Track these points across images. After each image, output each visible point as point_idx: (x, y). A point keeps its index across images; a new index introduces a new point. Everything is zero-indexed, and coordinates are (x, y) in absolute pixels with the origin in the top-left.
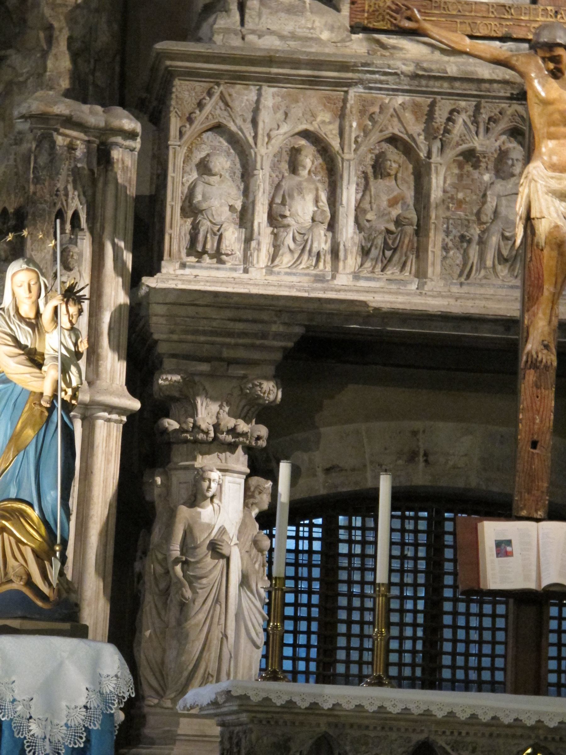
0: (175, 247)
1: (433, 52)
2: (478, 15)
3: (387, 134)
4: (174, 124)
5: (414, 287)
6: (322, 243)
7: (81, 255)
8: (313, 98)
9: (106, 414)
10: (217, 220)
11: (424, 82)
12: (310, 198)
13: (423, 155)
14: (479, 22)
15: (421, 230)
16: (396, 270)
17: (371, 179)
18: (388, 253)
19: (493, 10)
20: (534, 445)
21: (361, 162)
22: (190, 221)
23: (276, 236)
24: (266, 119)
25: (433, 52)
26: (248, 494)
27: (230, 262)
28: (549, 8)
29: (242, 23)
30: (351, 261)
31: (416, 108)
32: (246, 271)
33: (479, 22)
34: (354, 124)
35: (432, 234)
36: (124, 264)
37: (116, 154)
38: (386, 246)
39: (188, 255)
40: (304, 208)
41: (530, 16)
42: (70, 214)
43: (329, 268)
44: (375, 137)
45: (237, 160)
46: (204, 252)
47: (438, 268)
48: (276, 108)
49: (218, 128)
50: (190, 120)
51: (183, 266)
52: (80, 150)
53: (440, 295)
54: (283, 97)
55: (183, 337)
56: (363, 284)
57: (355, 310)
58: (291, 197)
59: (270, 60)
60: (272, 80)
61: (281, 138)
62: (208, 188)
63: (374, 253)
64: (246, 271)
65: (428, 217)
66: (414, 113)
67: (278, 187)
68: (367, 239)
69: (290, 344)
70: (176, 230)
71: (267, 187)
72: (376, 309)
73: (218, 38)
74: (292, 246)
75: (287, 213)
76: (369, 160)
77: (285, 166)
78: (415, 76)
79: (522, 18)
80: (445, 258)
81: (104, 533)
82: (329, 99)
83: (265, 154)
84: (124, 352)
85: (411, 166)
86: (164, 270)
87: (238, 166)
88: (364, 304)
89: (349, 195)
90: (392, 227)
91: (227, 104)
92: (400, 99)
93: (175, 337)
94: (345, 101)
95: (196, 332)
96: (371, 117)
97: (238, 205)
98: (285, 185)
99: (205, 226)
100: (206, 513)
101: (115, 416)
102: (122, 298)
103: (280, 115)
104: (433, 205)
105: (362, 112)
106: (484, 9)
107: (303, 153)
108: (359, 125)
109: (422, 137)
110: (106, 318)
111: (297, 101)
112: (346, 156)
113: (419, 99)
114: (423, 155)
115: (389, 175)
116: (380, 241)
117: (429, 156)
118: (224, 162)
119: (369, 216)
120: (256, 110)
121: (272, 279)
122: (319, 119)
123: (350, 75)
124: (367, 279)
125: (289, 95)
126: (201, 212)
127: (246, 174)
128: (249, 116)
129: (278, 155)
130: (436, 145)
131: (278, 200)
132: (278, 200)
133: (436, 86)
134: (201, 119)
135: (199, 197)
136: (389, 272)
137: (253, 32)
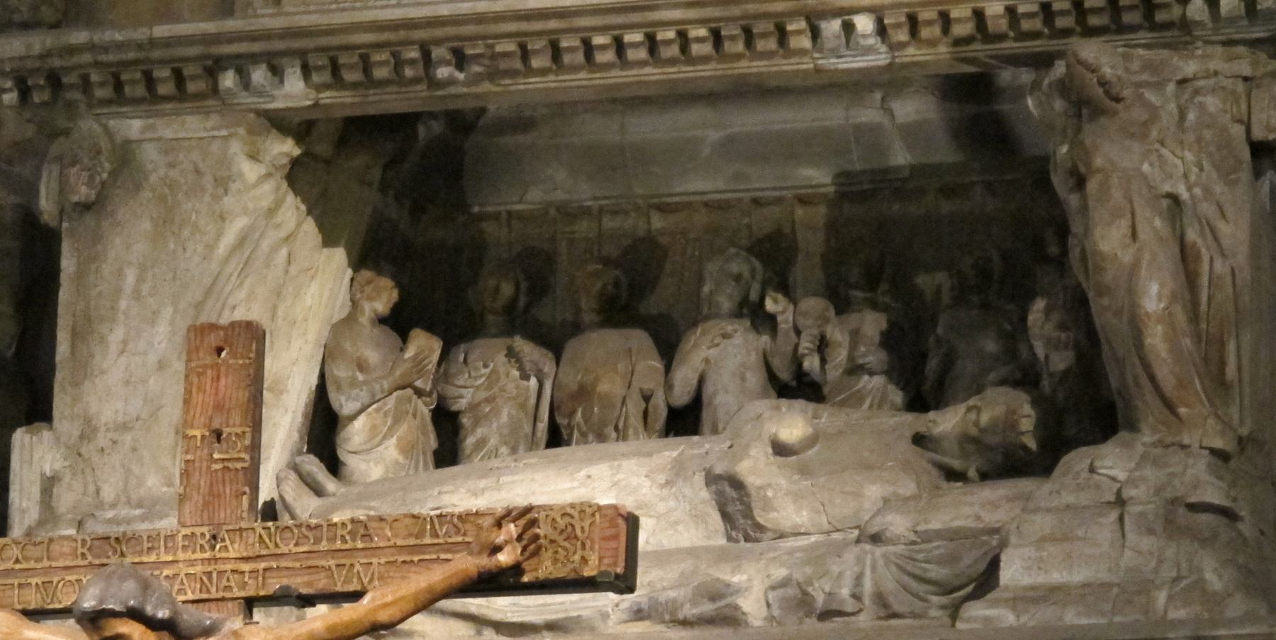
1: (479, 633)
2: (54, 564)
14: (55, 580)
19: (344, 533)
25: (479, 633)
28: (198, 531)
33: (55, 580)
41: (175, 554)
79: (145, 559)
106: (66, 549)
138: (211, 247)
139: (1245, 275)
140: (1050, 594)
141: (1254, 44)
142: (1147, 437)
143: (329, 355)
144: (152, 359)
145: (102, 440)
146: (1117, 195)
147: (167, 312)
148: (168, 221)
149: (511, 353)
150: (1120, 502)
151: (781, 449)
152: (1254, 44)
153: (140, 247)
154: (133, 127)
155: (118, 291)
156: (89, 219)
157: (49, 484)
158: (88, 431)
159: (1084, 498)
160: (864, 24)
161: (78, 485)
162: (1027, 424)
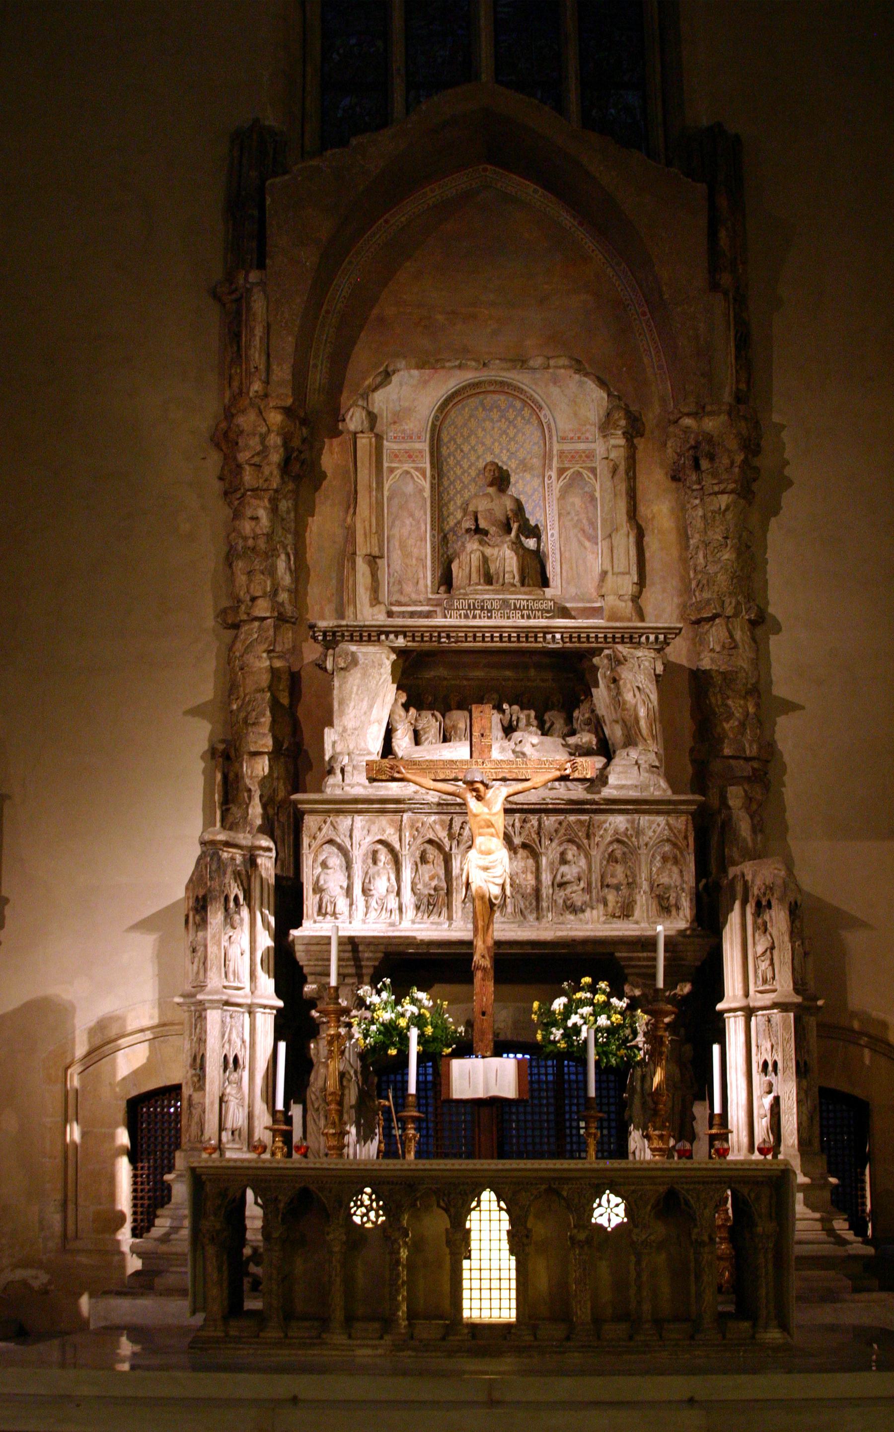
0: (310, 912)
3: (426, 838)
4: (306, 841)
5: (446, 926)
6: (393, 903)
8: (383, 821)
9: (262, 1010)
10: (333, 894)
11: (445, 807)
12: (385, 878)
13: (447, 849)
15: (449, 893)
16: (436, 917)
17: (419, 865)
18: (431, 908)
21: (413, 855)
22: (318, 896)
23: (367, 901)
24: (357, 834)
27: (341, 918)
29: (343, 780)
30: (410, 913)
31: (442, 822)
32: (350, 923)
34: (407, 834)
35: (454, 895)
36: (269, 923)
38: (429, 904)
39: (318, 915)
40: (382, 884)
43: (398, 917)
44: (420, 841)
45: (343, 859)
46: (326, 913)
47: (460, 914)
48: (363, 828)
49: (331, 842)
50: (315, 838)
51: (315, 922)
53: (460, 930)
54: (367, 821)
55: (316, 963)
56: (417, 926)
57: (409, 941)
58: (374, 878)
59: (356, 801)
60: (360, 812)
61: (366, 845)
62: (327, 876)
63: (422, 908)
64: (350, 923)
65: (452, 885)
66: (442, 825)
67: (367, 873)
68: (419, 900)
69: (377, 964)
70: (310, 901)
71: (361, 874)
72: (421, 940)
73: (328, 790)
74: (376, 907)
75: (372, 888)
76: (418, 854)
77: (370, 861)
78: (439, 804)
80: (464, 908)
82: (392, 820)
83: (358, 855)
84: (272, 974)
85: (442, 857)
86: (304, 925)
87: (344, 862)
88: (414, 938)
89: (407, 874)
90: (432, 892)
91: (334, 827)
92: (433, 818)
93: (312, 963)
94: (401, 821)
96: (417, 830)
97: (345, 885)
98: (371, 872)
99: (326, 898)
101: (268, 1011)
102: (271, 943)
103: (365, 832)
104: (454, 878)
105: (412, 827)
107: (379, 853)
108: (410, 834)
109: (447, 839)
111: (374, 823)
112: (404, 853)
113: (444, 817)
114: (447, 849)
115: (428, 862)
116: (425, 901)
117: (451, 849)
118: (336, 861)
119: (419, 887)
120: (351, 830)
121: (365, 926)
122: (387, 832)
123: (402, 806)
124: (420, 923)
125: (370, 820)
126: (324, 890)
127: (349, 867)
128: (348, 834)
129: (366, 855)
130: (455, 843)
131: (367, 881)
132: (367, 881)
133: (452, 809)
134: (321, 837)
135: (322, 882)
136: (432, 918)
137: (349, 785)
138: (378, 682)
139: (657, 708)
140: (622, 787)
141: (654, 649)
142: (640, 747)
144: (363, 711)
145: (349, 732)
146: (629, 686)
147: (366, 699)
148: (365, 675)
149: (433, 715)
150: (637, 763)
151: (533, 746)
152: (654, 649)
153: (357, 681)
155: (351, 692)
156: (342, 672)
157: (334, 743)
158: (345, 730)
159: (628, 763)
161: (342, 744)
162: (594, 743)
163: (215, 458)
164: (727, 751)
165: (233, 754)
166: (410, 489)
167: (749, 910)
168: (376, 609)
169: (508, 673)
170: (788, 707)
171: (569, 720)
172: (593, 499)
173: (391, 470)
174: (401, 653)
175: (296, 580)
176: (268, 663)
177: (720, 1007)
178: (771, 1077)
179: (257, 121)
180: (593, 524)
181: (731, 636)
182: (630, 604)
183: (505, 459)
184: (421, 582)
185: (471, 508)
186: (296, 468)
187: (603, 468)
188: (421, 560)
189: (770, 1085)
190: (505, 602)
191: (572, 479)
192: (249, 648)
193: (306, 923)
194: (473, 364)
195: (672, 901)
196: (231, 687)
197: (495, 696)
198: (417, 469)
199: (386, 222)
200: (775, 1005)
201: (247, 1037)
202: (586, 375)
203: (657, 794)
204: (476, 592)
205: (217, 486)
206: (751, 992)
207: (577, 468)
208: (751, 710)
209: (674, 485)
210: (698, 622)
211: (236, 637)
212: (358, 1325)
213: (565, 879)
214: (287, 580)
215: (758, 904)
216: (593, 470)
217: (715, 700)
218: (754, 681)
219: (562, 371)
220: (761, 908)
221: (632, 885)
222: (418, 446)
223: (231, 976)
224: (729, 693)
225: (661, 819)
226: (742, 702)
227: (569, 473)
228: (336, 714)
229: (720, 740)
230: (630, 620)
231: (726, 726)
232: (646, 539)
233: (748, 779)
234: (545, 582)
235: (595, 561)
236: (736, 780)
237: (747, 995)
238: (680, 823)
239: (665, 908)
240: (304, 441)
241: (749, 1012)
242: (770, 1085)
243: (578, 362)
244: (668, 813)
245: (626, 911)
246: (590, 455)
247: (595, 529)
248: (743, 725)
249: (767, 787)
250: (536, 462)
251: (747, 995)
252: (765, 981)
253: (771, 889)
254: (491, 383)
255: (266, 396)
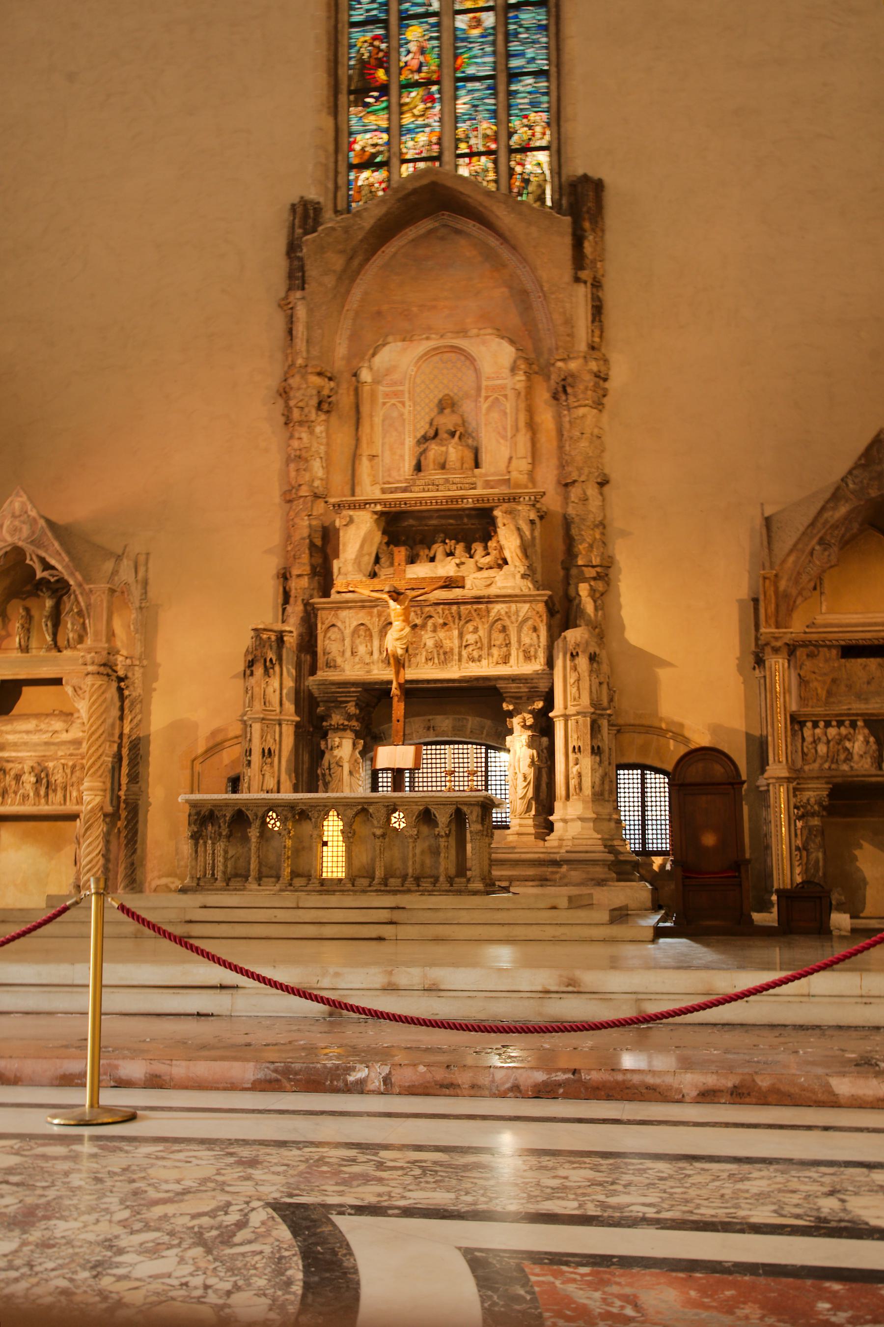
7: (274, 672)
20: (398, 721)
26: (354, 745)
37: (285, 638)
42: (268, 660)
49: (333, 625)
52: (273, 638)
81: (288, 761)
95: (327, 693)
100: (336, 752)
110: (285, 691)
127: (343, 640)
140: (504, 588)
143: (379, 548)
154: (351, 513)
157: (340, 568)
160: (470, 500)
163: (280, 402)
164: (580, 563)
165: (288, 576)
166: (395, 414)
167: (568, 656)
168: (374, 487)
169: (451, 521)
170: (624, 534)
171: (486, 548)
172: (505, 413)
173: (384, 404)
174: (382, 514)
175: (328, 473)
176: (307, 523)
177: (551, 715)
178: (578, 755)
179: (302, 198)
180: (505, 429)
181: (585, 493)
182: (526, 476)
183: (456, 391)
184: (402, 469)
185: (435, 423)
186: (325, 407)
187: (511, 395)
188: (402, 457)
189: (577, 759)
190: (447, 481)
191: (493, 403)
192: (297, 514)
193: (319, 673)
194: (433, 336)
195: (532, 653)
196: (288, 538)
197: (442, 535)
198: (400, 402)
199: (383, 252)
200: (578, 713)
201: (277, 738)
202: (503, 338)
203: (526, 591)
204: (431, 475)
205: (282, 420)
206: (569, 706)
207: (496, 395)
208: (598, 536)
209: (555, 402)
210: (566, 485)
211: (291, 508)
212: (264, 879)
213: (469, 643)
214: (320, 473)
215: (572, 654)
216: (505, 396)
217: (574, 532)
218: (600, 519)
219: (488, 337)
220: (573, 656)
221: (508, 645)
222: (400, 388)
223: (267, 704)
224: (583, 527)
225: (527, 606)
226: (591, 532)
227: (491, 399)
228: (341, 551)
229: (576, 556)
230: (526, 487)
231: (581, 547)
232: (538, 436)
233: (594, 579)
234: (477, 465)
235: (505, 452)
236: (585, 580)
237: (566, 708)
238: (541, 607)
239: (528, 657)
240: (331, 390)
241: (566, 718)
242: (577, 759)
243: (498, 330)
244: (530, 602)
245: (506, 660)
246: (503, 387)
247: (506, 432)
248: (591, 546)
249: (608, 584)
250: (473, 392)
251: (566, 708)
252: (575, 699)
253: (578, 645)
254: (445, 347)
255: (306, 366)
